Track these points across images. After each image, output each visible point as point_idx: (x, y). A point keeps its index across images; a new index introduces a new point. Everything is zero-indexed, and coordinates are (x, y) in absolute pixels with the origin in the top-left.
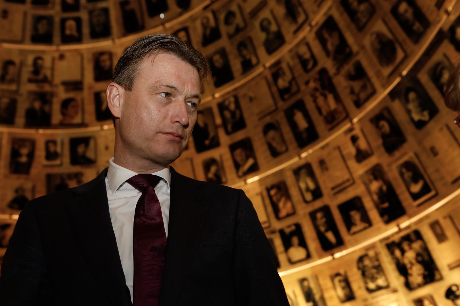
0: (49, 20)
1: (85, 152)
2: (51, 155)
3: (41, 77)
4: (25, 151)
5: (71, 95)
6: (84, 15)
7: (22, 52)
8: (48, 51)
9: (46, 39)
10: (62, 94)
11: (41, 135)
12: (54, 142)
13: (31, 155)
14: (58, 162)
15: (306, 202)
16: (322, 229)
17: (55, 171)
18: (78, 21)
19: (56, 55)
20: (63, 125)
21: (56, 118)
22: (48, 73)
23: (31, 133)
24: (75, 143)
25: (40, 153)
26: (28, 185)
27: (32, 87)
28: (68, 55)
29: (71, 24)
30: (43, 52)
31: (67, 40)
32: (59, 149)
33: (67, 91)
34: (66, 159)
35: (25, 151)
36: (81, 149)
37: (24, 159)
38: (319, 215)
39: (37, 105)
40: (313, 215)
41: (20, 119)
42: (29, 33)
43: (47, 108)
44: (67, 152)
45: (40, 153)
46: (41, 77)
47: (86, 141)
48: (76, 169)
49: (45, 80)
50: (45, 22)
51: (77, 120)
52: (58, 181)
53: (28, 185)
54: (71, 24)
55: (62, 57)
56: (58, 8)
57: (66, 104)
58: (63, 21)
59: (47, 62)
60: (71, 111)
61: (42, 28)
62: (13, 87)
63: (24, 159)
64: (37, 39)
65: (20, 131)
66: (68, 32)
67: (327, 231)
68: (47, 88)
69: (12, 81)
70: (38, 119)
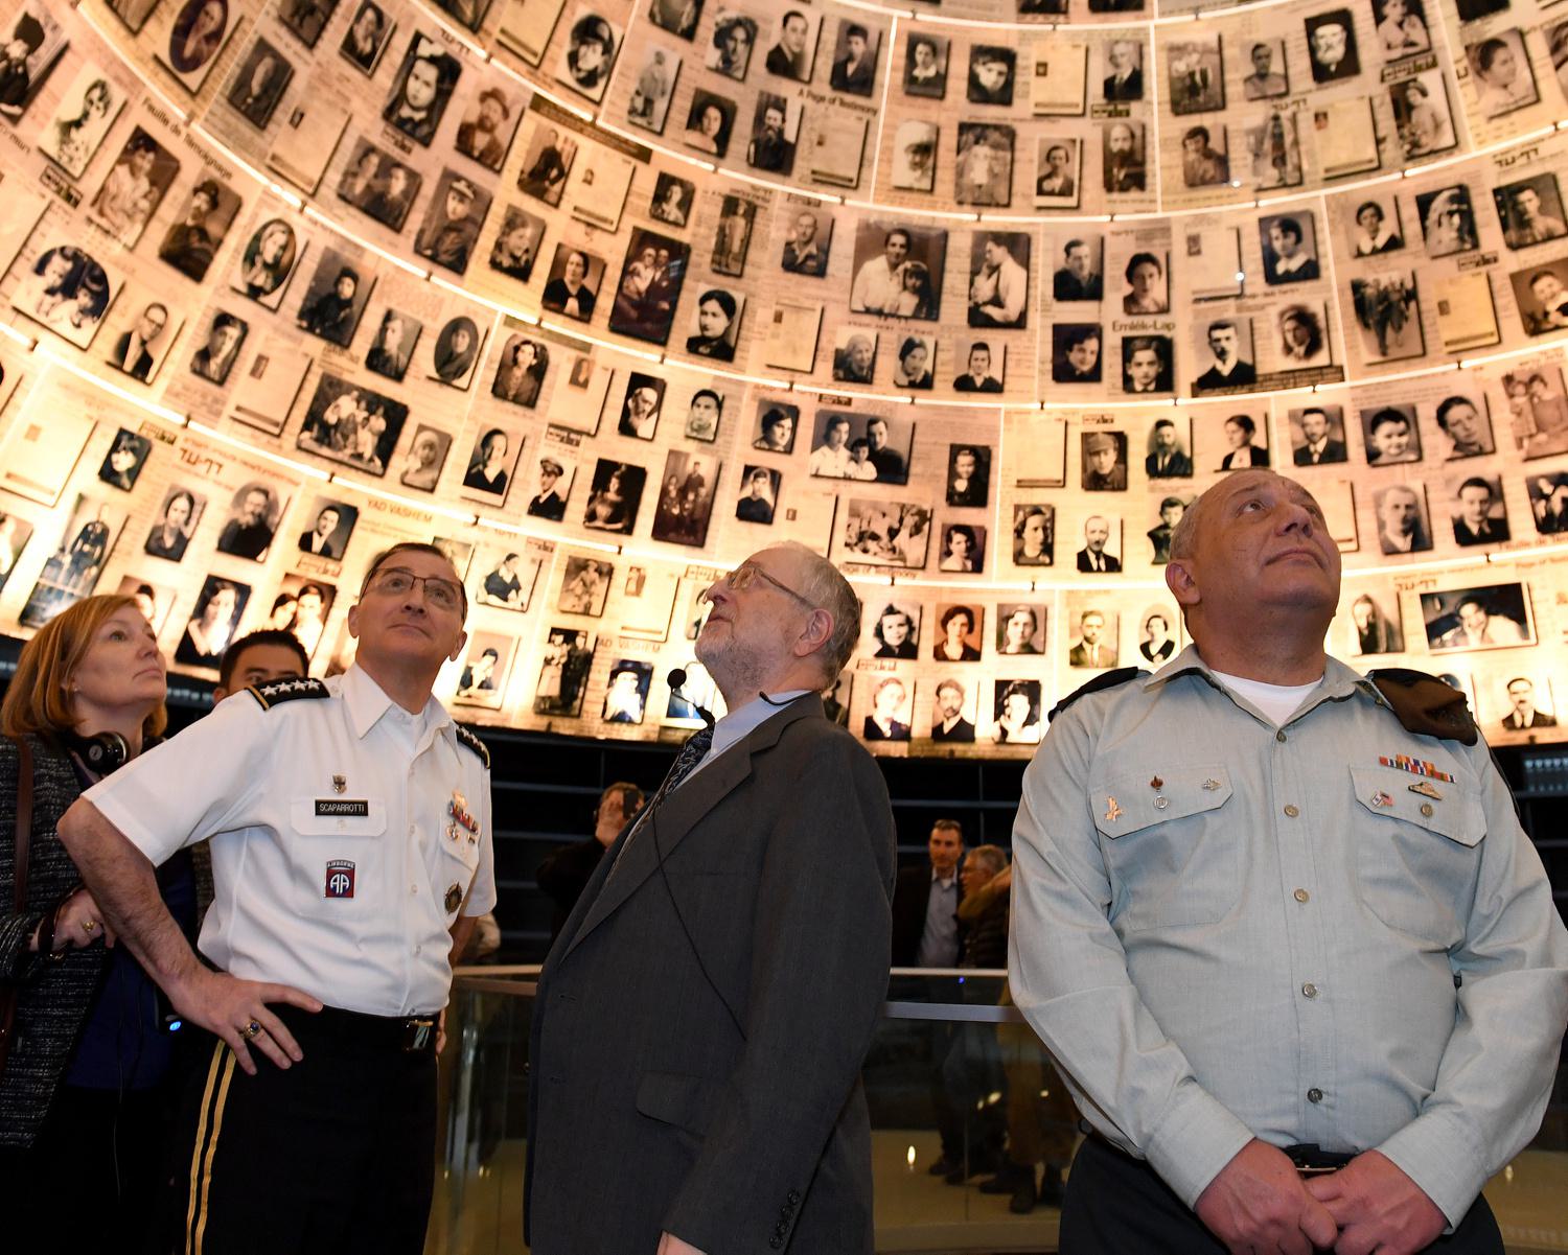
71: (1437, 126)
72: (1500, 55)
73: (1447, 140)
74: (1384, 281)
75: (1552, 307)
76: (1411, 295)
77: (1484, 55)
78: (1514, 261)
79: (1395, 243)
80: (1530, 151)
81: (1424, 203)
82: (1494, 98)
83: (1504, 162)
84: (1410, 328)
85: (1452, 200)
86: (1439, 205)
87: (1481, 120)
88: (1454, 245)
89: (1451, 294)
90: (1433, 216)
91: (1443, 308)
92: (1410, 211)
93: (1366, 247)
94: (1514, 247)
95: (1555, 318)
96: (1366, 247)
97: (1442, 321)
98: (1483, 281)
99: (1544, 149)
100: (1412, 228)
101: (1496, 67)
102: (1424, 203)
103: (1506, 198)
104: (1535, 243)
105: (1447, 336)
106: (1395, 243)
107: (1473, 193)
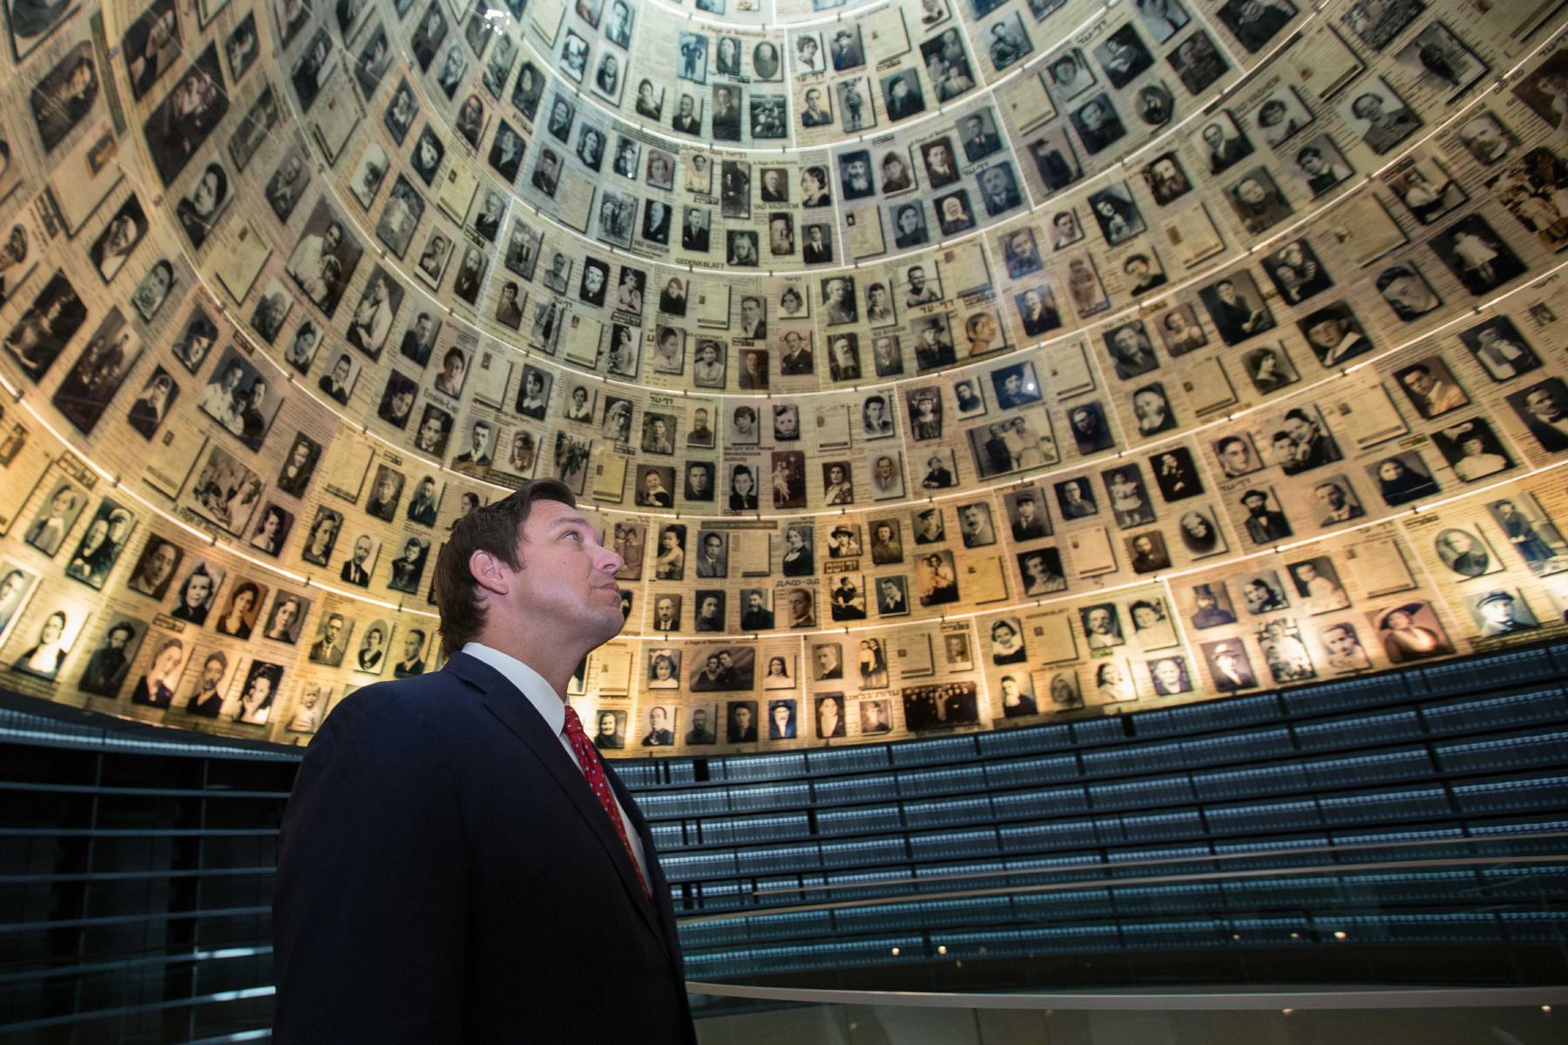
0: (917, 208)
1: (1019, 387)
2: (966, 404)
3: (924, 295)
4: (927, 407)
5: (977, 310)
6: (969, 184)
7: (888, 267)
8: (926, 255)
9: (916, 238)
10: (964, 312)
11: (943, 379)
12: (968, 384)
13: (938, 410)
14: (980, 410)
15: (1494, 379)
16: (1545, 418)
17: (979, 423)
18: (962, 196)
19: (940, 256)
20: (973, 356)
21: (962, 350)
22: (935, 287)
23: (932, 378)
24: (999, 377)
25: (951, 403)
26: (945, 452)
27: (917, 313)
28: (957, 251)
29: (951, 204)
30: (920, 257)
31: (949, 229)
32: (977, 393)
33: (969, 305)
34: (993, 404)
35: (927, 407)
36: (1011, 384)
37: (929, 418)
38: (1533, 398)
39: (929, 337)
40: (1518, 402)
41: (911, 364)
42: (891, 238)
43: (945, 338)
44: (990, 393)
45: (951, 403)
46: (924, 295)
47: (1017, 370)
48: (1012, 413)
49: (932, 298)
50: (910, 212)
51: (997, 343)
52: (988, 438)
53: (945, 452)
54: (951, 204)
55: (949, 257)
56: (925, 185)
57: (973, 323)
58: (938, 203)
59: (929, 272)
60: (983, 332)
61: (909, 224)
62: (890, 321)
63: (929, 418)
64: (904, 242)
65: (914, 379)
66: (949, 218)
67: (1554, 420)
68: (938, 309)
69: (884, 313)
70: (937, 357)
71: (630, 361)
72: (672, 339)
73: (632, 372)
74: (575, 440)
75: (652, 492)
76: (586, 455)
77: (666, 333)
78: (642, 458)
79: (587, 419)
80: (669, 399)
81: (610, 402)
82: (661, 361)
83: (655, 398)
84: (579, 474)
85: (623, 407)
86: (616, 408)
87: (651, 369)
88: (616, 435)
89: (605, 462)
90: (611, 412)
91: (600, 470)
92: (601, 404)
93: (573, 415)
94: (645, 450)
95: (652, 499)
96: (573, 415)
97: (597, 477)
98: (623, 463)
99: (677, 402)
100: (599, 415)
101: (668, 344)
102: (610, 402)
103: (652, 419)
104: (655, 452)
105: (596, 488)
106: (587, 419)
107: (635, 409)
